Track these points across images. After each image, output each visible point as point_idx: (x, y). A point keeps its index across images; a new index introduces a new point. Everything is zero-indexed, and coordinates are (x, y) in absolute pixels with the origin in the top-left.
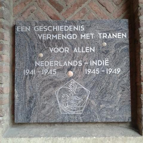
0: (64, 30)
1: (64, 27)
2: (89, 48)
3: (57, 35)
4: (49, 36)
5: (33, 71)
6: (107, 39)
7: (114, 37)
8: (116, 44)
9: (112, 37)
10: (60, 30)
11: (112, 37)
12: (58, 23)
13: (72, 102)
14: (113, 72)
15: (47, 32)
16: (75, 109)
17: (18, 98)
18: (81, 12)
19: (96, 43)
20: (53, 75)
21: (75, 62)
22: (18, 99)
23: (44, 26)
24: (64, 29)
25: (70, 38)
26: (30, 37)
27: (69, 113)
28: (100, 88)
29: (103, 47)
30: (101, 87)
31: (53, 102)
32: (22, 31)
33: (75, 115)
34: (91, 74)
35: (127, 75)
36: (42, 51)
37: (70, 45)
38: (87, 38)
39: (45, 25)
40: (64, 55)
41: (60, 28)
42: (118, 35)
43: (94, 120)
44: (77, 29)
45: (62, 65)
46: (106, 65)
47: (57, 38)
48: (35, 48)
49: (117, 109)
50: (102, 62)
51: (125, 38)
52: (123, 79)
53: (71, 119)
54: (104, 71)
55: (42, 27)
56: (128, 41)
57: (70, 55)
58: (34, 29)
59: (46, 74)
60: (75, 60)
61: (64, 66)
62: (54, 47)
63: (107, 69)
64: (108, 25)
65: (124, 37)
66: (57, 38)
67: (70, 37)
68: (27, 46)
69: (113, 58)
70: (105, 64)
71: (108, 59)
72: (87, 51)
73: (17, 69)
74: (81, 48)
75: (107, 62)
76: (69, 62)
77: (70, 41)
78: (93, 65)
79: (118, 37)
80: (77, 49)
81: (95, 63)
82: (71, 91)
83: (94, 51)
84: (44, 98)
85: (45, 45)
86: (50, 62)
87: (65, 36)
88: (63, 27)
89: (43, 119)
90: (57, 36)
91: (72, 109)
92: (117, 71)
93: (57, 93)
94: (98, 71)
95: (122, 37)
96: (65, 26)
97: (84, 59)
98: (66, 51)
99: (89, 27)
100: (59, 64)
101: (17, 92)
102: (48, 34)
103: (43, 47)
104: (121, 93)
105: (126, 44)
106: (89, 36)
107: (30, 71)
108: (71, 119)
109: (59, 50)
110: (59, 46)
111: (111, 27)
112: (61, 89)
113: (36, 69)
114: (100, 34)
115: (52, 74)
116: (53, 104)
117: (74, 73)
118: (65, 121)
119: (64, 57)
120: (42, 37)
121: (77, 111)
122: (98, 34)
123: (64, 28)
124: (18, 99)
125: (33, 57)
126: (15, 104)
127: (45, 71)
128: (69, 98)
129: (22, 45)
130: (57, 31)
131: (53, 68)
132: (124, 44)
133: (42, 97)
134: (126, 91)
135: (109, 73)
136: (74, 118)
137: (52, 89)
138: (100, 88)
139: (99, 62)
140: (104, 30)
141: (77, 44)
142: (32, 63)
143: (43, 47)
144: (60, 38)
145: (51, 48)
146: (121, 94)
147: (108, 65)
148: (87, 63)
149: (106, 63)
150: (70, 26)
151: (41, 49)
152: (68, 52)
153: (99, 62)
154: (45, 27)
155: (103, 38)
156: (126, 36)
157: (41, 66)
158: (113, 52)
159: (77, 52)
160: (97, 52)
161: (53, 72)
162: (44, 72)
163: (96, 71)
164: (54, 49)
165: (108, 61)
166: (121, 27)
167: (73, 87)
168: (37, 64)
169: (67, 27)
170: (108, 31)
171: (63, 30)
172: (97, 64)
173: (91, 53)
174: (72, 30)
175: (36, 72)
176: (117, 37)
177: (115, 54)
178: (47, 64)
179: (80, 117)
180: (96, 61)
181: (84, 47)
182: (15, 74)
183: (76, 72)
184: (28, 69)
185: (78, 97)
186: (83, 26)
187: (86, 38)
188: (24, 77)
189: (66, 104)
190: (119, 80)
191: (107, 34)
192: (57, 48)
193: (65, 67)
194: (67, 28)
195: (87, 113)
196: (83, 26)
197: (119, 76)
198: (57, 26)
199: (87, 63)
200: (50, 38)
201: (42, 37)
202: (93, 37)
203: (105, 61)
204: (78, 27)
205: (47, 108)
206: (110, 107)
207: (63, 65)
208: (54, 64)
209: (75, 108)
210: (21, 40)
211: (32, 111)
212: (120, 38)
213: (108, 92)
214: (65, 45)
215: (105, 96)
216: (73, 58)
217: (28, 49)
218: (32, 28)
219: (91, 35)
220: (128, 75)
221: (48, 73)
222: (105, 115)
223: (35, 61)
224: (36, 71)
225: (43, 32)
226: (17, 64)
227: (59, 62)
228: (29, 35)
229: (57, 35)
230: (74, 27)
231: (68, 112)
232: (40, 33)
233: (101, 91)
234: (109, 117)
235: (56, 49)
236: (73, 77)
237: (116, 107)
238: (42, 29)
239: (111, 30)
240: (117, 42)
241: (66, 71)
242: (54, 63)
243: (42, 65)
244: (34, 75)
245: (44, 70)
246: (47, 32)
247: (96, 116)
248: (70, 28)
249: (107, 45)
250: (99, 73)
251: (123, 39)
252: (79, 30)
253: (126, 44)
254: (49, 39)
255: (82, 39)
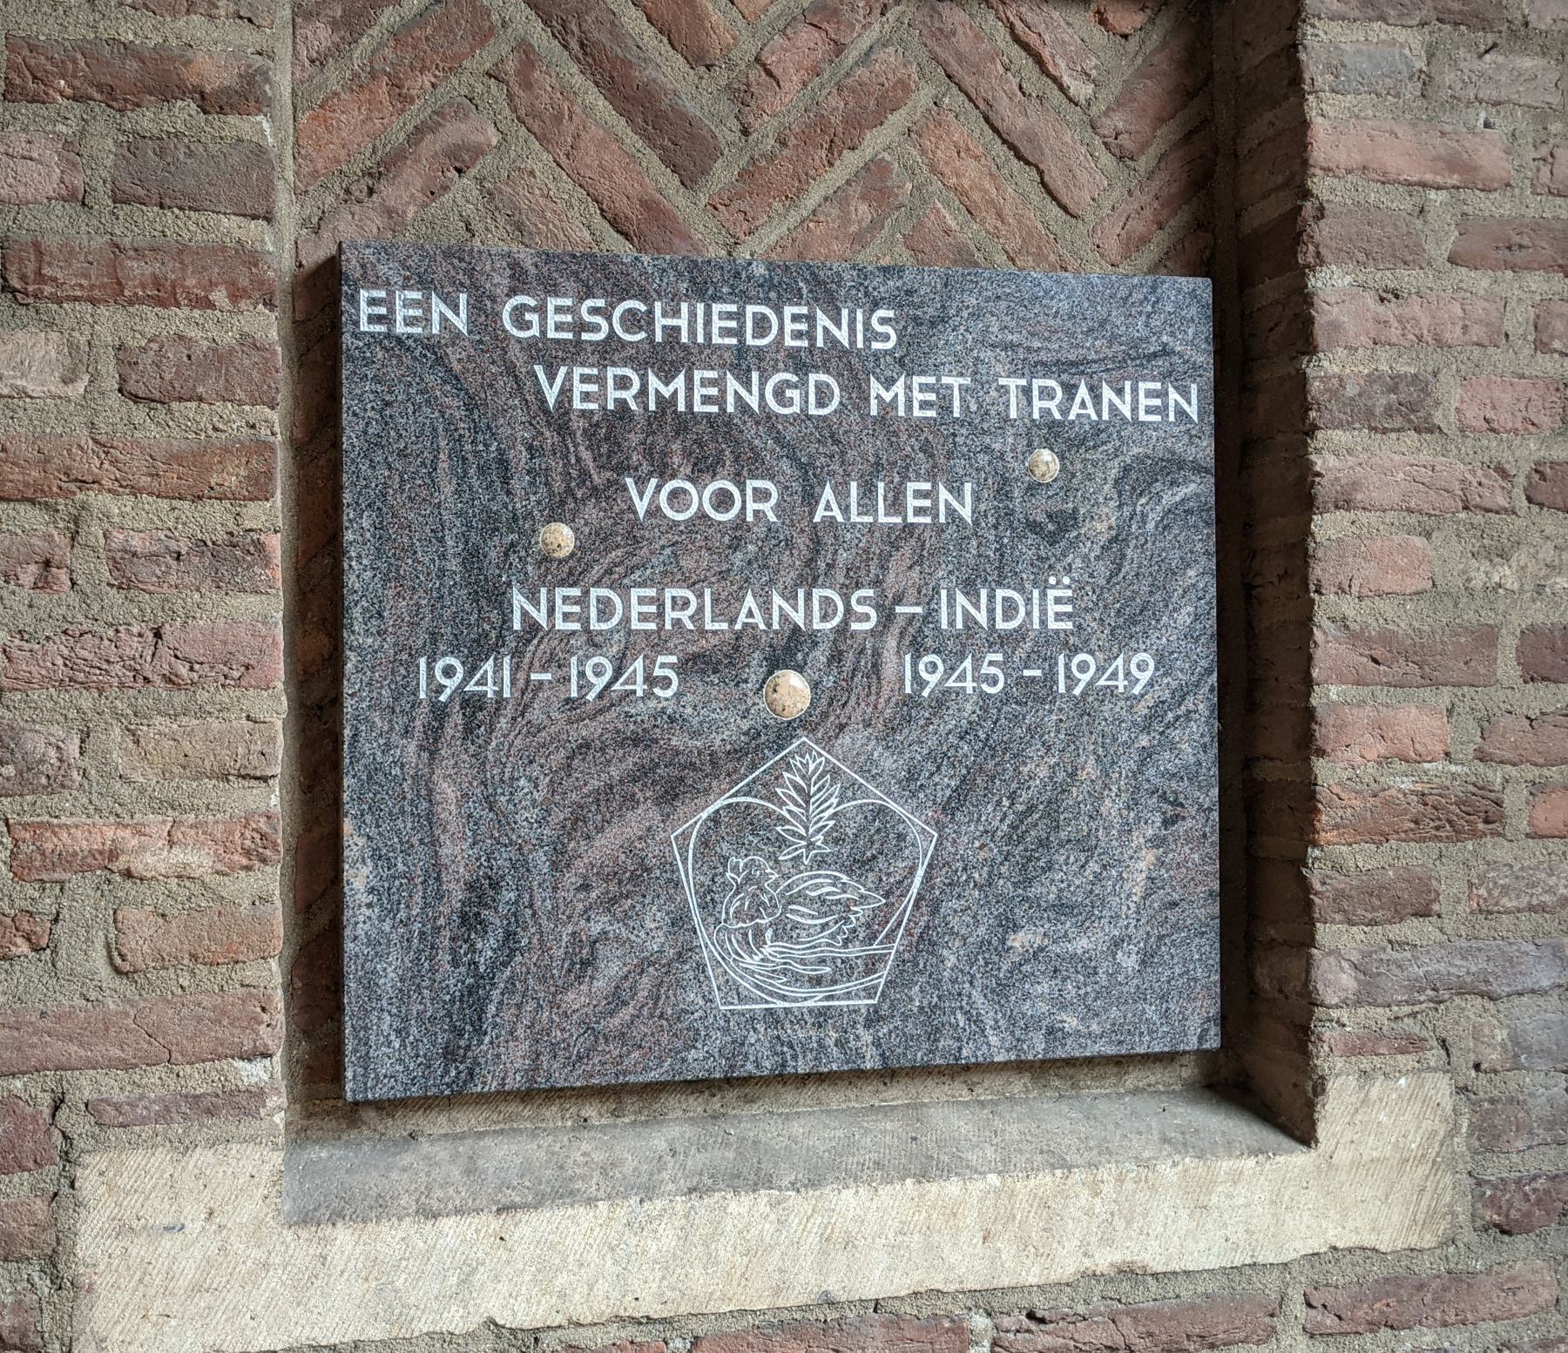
0: (742, 342)
1: (739, 316)
2: (927, 486)
3: (689, 380)
4: (623, 383)
5: (498, 668)
6: (1060, 424)
7: (1113, 409)
8: (1126, 470)
9: (1099, 413)
10: (708, 335)
11: (1099, 413)
12: (693, 281)
13: (802, 915)
14: (1102, 682)
15: (609, 350)
16: (827, 970)
17: (371, 891)
18: (856, 190)
19: (987, 449)
20: (652, 704)
21: (827, 601)
22: (369, 905)
23: (581, 300)
24: (739, 333)
25: (791, 402)
26: (472, 382)
27: (780, 1004)
28: (1006, 802)
29: (1032, 489)
30: (1012, 797)
31: (654, 918)
32: (400, 329)
33: (822, 1017)
34: (948, 691)
35: (1201, 706)
36: (563, 503)
37: (785, 465)
38: (917, 413)
39: (590, 294)
40: (736, 545)
41: (708, 323)
42: (1144, 402)
43: (965, 1053)
44: (842, 336)
45: (725, 626)
46: (1053, 625)
47: (689, 404)
48: (506, 481)
49: (1129, 961)
50: (1029, 601)
51: (1191, 421)
52: (1175, 734)
53: (792, 1047)
54: (1037, 673)
55: (568, 302)
56: (1205, 450)
57: (789, 544)
58: (498, 315)
59: (600, 696)
60: (823, 586)
61: (738, 627)
62: (661, 475)
63: (1061, 660)
64: (1072, 317)
65: (1181, 413)
66: (689, 404)
67: (788, 393)
68: (444, 465)
69: (1102, 569)
70: (1043, 622)
71: (1066, 581)
72: (919, 511)
73: (359, 649)
74: (868, 490)
75: (1058, 601)
76: (777, 600)
77: (790, 433)
78: (959, 625)
79: (1143, 417)
80: (841, 494)
81: (977, 606)
82: (794, 834)
83: (966, 513)
84: (586, 887)
85: (586, 455)
86: (634, 601)
87: (747, 385)
88: (729, 316)
89: (580, 1058)
90: (690, 389)
91: (799, 968)
92: (1128, 674)
93: (683, 849)
94: (993, 670)
95: (1172, 418)
96: (751, 309)
97: (891, 578)
98: (756, 513)
99: (933, 324)
100: (700, 609)
101: (361, 841)
102: (614, 364)
103: (574, 473)
104: (1157, 842)
105: (1198, 469)
106: (932, 397)
107: (470, 673)
108: (792, 1047)
109: (701, 498)
110: (703, 469)
111: (1091, 330)
112: (715, 819)
113: (517, 654)
114: (1013, 383)
115: (649, 695)
116: (652, 931)
117: (815, 686)
118: (750, 1067)
119: (739, 555)
120: (566, 392)
121: (839, 989)
122: (1002, 381)
123: (742, 326)
124: (369, 905)
125: (493, 554)
126: (349, 946)
127: (595, 672)
128: (776, 885)
129: (402, 454)
130: (685, 347)
131: (657, 642)
132: (1181, 464)
133: (571, 879)
134: (1189, 823)
135: (1077, 691)
136: (819, 1042)
137: (643, 816)
138: (1006, 802)
139: (1004, 599)
140: (1043, 356)
141: (843, 453)
142: (483, 602)
143: (574, 473)
144: (707, 400)
145: (641, 482)
146: (1158, 847)
147: (1069, 625)
148: (918, 610)
149: (1051, 614)
150: (789, 311)
151: (558, 486)
152: (772, 518)
153: (1004, 599)
154: (589, 303)
155: (1036, 416)
156: (1193, 411)
157: (560, 625)
158: (1100, 528)
159: (840, 519)
160: (992, 520)
161: (650, 680)
162: (582, 674)
163: (985, 670)
164: (658, 488)
165: (1069, 593)
166: (1165, 338)
167: (807, 798)
168: (525, 614)
169: (764, 318)
170: (1073, 364)
171: (734, 341)
172: (992, 619)
173: (941, 530)
174: (805, 343)
175: (521, 676)
176: (1134, 409)
177: (1114, 540)
178: (605, 610)
179: (861, 1031)
180: (984, 593)
181: (897, 479)
182: (347, 690)
183: (829, 682)
184: (454, 650)
185: (845, 879)
186: (891, 314)
187: (909, 407)
188: (421, 718)
189: (759, 932)
190: (1144, 741)
191: (1062, 384)
192: (688, 486)
193: (745, 642)
194: (761, 325)
195: (911, 1000)
196: (891, 314)
197: (1142, 709)
198: (684, 307)
199: (918, 610)
200: (628, 395)
201: (566, 392)
202: (965, 408)
203: (1043, 595)
204: (852, 321)
205: (611, 968)
206: (1082, 944)
207: (732, 621)
208: (660, 614)
209: (822, 961)
210: (388, 404)
211: (488, 996)
212: (1156, 418)
213: (1063, 835)
214: (748, 464)
215: (1041, 863)
216: (810, 563)
217: (448, 489)
218: (483, 309)
219: (949, 387)
220: (1202, 703)
221: (617, 686)
222: (1043, 1007)
223: (509, 584)
224: (515, 669)
225: (573, 351)
226: (356, 612)
227: (700, 596)
228: (457, 367)
229: (689, 380)
230: (823, 320)
231: (771, 994)
232: (550, 354)
233: (1013, 827)
234: (1071, 1022)
235: (675, 494)
236: (805, 723)
237: (1117, 943)
238: (569, 318)
239: (1093, 356)
240: (1136, 450)
241: (754, 674)
242: (661, 606)
243: (567, 617)
244: (500, 701)
245: (581, 663)
246: (609, 350)
247: (978, 1021)
248: (789, 326)
249: (1063, 469)
250: (1001, 685)
251: (1176, 430)
252: (860, 345)
253: (1198, 469)
254: (622, 403)
255: (882, 420)
